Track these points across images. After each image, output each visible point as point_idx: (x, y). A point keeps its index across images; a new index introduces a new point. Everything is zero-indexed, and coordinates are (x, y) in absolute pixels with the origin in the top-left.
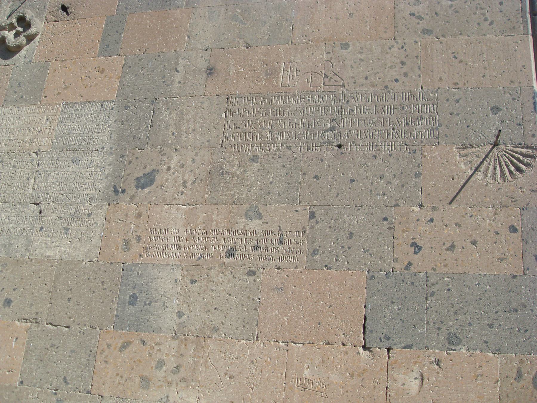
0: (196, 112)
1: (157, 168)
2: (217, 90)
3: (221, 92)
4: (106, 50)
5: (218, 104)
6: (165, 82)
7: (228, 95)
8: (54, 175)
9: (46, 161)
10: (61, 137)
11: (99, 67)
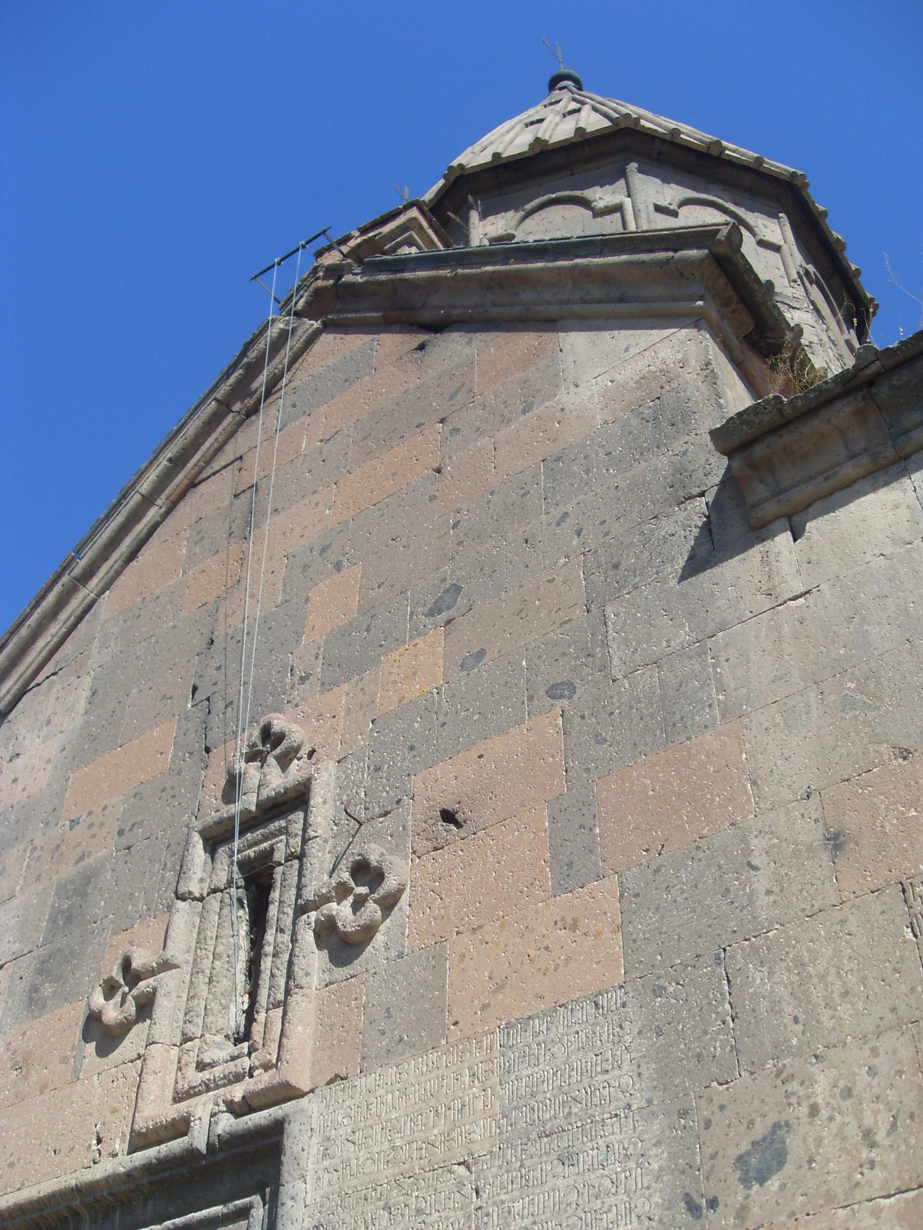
0: (834, 949)
1: (783, 1118)
2: (869, 879)
3: (881, 881)
4: (568, 876)
5: (884, 912)
6: (732, 903)
7: (901, 883)
8: (524, 1208)
9: (493, 1177)
10: (516, 1108)
11: (563, 919)
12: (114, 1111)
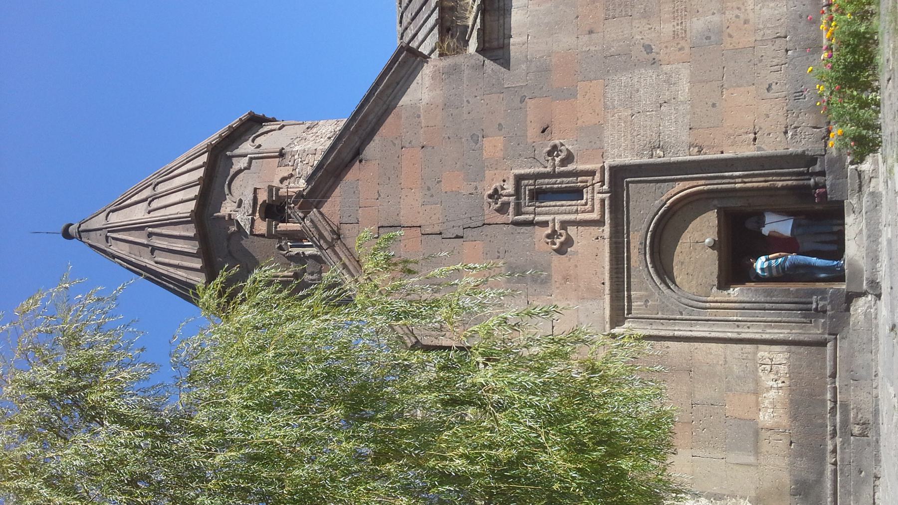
12: (591, 234)
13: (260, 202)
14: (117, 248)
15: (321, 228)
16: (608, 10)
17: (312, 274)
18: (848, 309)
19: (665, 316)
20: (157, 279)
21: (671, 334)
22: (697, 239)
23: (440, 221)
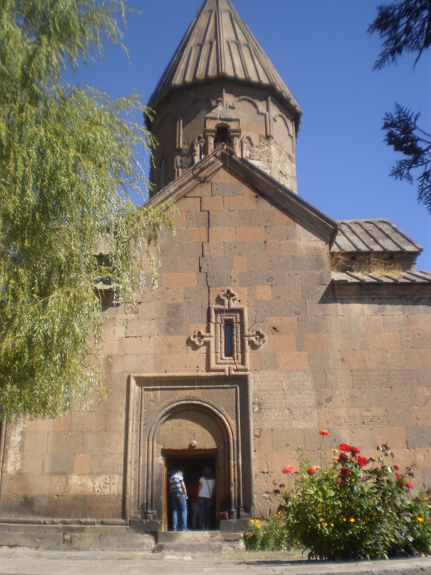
13: (230, 124)
14: (203, 18)
15: (209, 168)
16: (358, 371)
17: (181, 161)
18: (146, 532)
19: (143, 414)
20: (180, 48)
21: (131, 417)
22: (196, 435)
23: (212, 255)
